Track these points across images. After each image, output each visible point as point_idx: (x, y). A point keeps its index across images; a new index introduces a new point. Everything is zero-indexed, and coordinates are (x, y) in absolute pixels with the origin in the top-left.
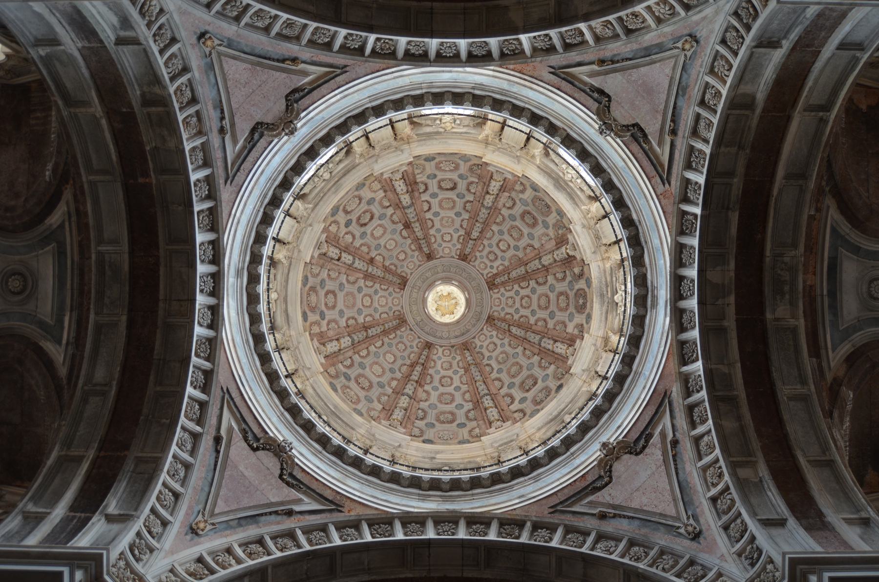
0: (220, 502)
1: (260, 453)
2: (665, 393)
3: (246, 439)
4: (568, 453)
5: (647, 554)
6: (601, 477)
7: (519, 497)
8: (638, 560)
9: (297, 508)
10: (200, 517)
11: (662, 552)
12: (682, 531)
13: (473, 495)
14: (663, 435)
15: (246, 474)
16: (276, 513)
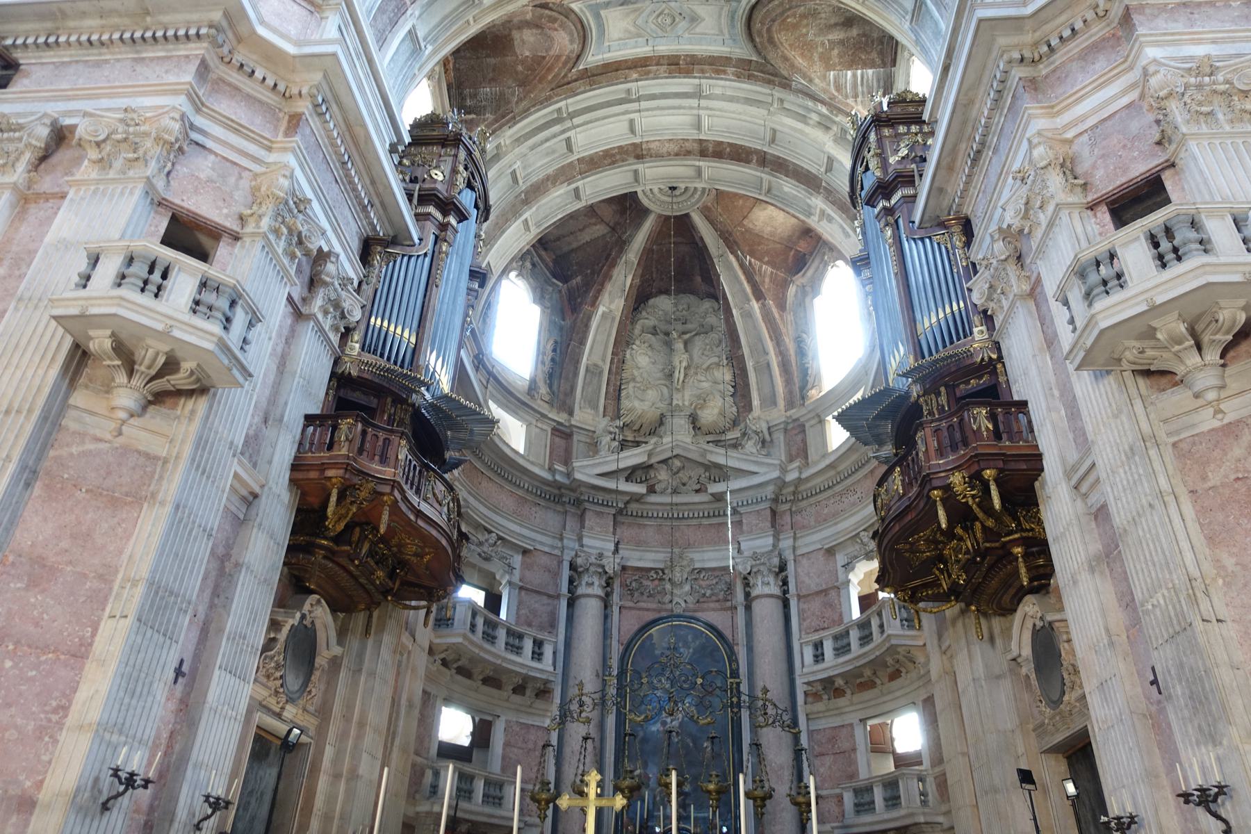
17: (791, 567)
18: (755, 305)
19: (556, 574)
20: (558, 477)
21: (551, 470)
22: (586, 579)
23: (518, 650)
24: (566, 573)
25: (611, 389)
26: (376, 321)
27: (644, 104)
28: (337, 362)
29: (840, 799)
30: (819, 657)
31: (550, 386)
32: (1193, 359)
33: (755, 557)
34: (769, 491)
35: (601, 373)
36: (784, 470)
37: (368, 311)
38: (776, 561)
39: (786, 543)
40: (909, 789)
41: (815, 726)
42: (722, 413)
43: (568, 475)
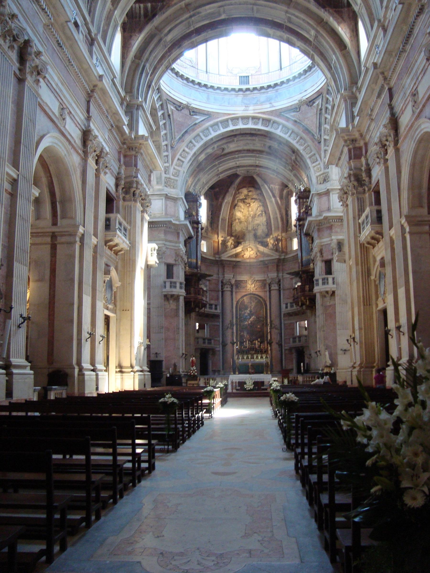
0: (176, 134)
1: (183, 111)
2: (321, 93)
3: (177, 109)
4: (288, 85)
5: (304, 144)
6: (296, 108)
7: (271, 103)
8: (301, 145)
9: (197, 122)
10: (172, 142)
11: (308, 146)
12: (316, 138)
13: (254, 94)
14: (318, 105)
15: (180, 120)
16: (192, 126)
17: (282, 281)
18: (273, 199)
19: (217, 285)
20: (217, 259)
21: (214, 257)
22: (226, 286)
23: (211, 308)
24: (220, 285)
25: (229, 224)
26: (189, 260)
27: (240, 159)
28: (185, 272)
29: (290, 339)
30: (287, 307)
31: (211, 227)
32: (327, 295)
33: (272, 279)
34: (276, 261)
35: (226, 220)
36: (280, 256)
37: (188, 258)
38: (277, 280)
39: (280, 275)
40: (303, 339)
41: (286, 322)
42: (263, 231)
43: (220, 258)
